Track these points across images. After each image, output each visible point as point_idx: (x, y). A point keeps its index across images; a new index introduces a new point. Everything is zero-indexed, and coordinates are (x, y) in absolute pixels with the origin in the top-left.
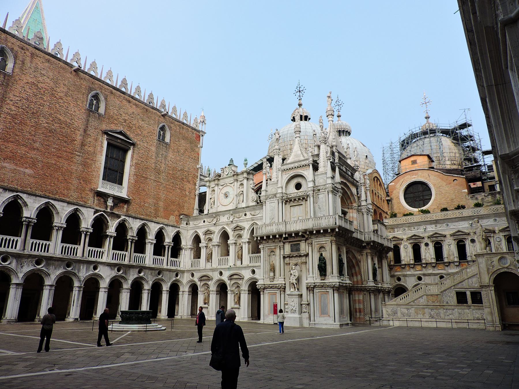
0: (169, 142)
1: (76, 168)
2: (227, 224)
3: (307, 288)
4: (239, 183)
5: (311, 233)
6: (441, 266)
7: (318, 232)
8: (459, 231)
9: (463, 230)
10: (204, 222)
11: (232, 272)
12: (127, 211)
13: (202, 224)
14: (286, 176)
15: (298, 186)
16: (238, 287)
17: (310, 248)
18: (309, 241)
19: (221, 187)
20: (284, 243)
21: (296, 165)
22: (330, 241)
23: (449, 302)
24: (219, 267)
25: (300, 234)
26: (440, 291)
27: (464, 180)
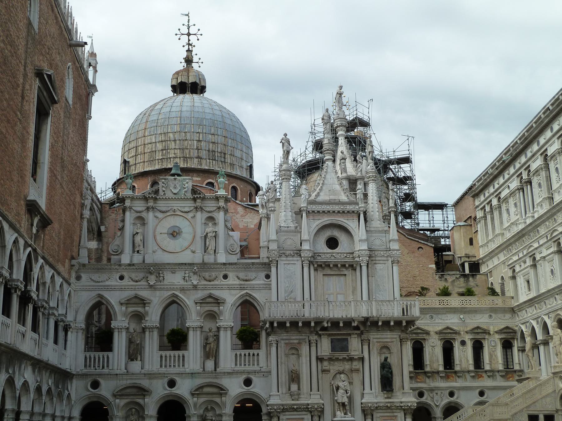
0: (71, 103)
1: (17, 146)
2: (183, 290)
3: (363, 411)
4: (206, 215)
5: (374, 324)
6: (421, 377)
7: (386, 323)
8: (448, 328)
9: (451, 327)
10: (122, 278)
11: (199, 381)
12: (43, 247)
13: (114, 281)
14: (317, 223)
15: (332, 243)
16: (212, 409)
17: (366, 347)
18: (364, 337)
19: (160, 215)
20: (320, 336)
21: (336, 208)
22: (398, 339)
24: (163, 370)
25: (356, 325)
26: (511, 414)
27: (432, 250)
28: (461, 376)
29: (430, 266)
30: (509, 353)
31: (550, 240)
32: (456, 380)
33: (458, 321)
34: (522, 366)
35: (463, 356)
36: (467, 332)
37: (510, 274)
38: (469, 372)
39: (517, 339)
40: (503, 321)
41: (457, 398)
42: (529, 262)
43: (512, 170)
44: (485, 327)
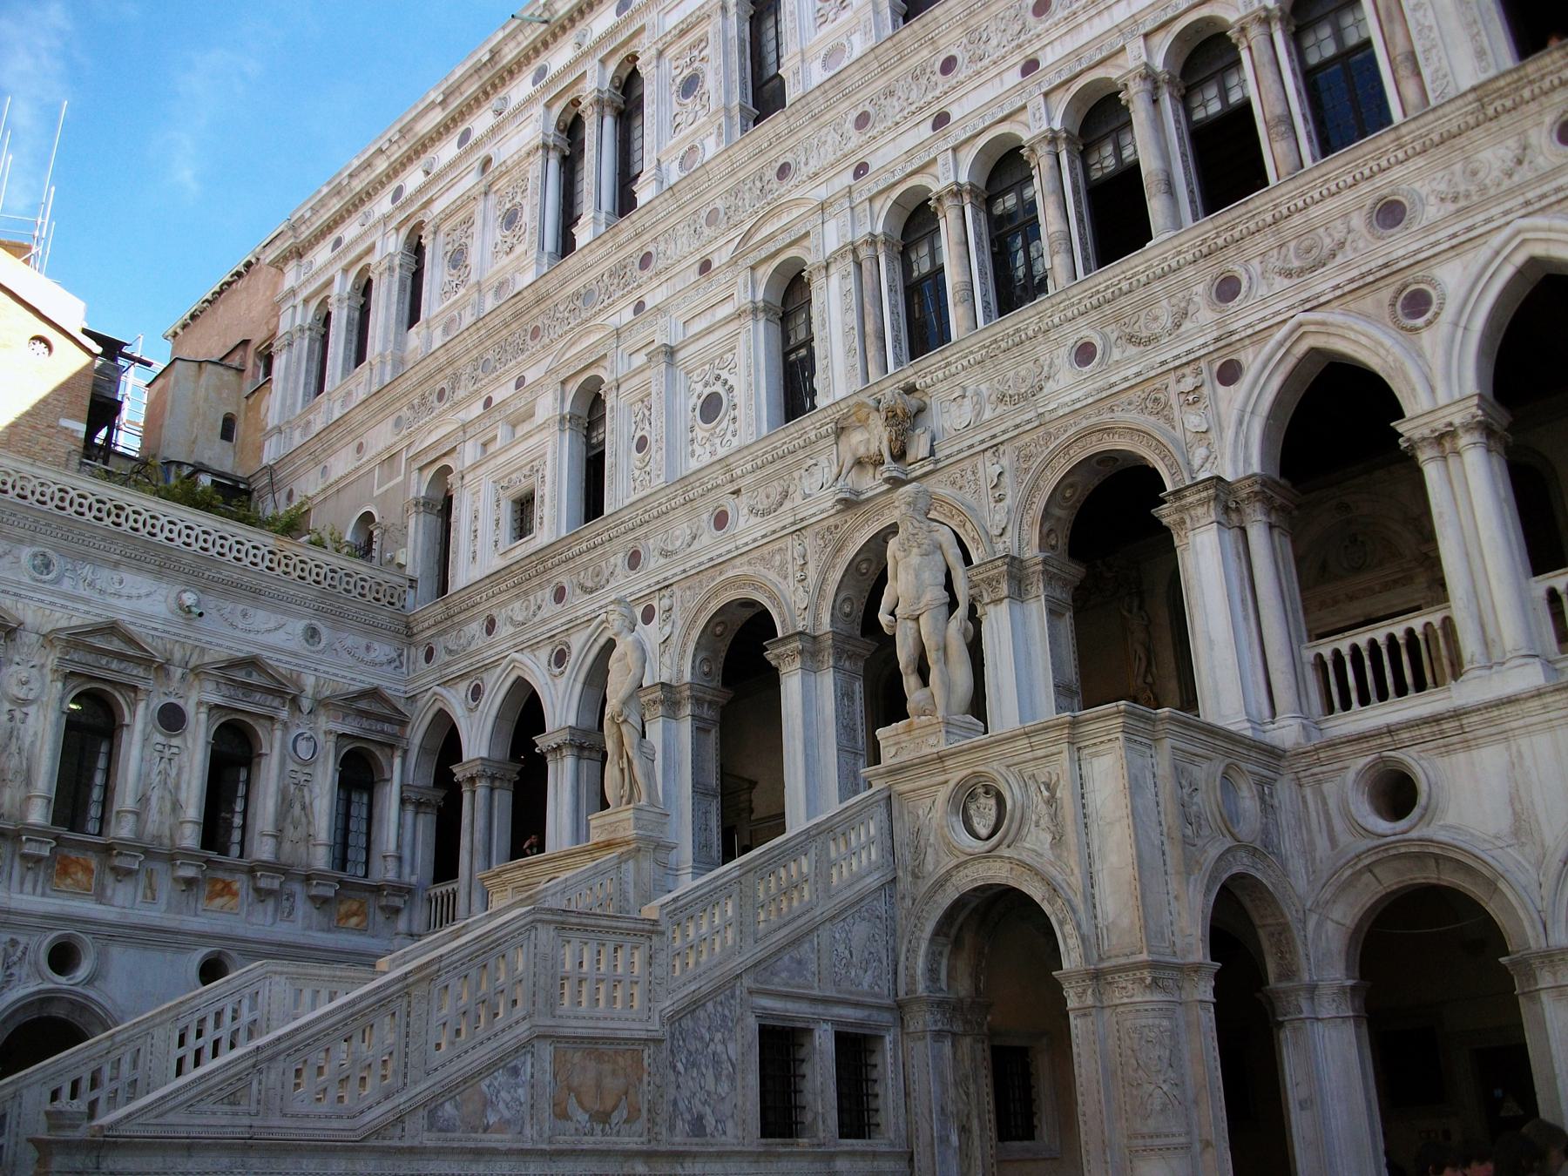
23: (710, 1121)
26: (667, 1004)
28: (129, 873)
29: (65, 423)
30: (358, 810)
31: (733, 261)
32: (103, 888)
33: (169, 616)
34: (407, 870)
35: (159, 776)
36: (198, 672)
37: (419, 486)
38: (172, 857)
39: (405, 752)
40: (362, 667)
41: (89, 981)
42: (548, 406)
43: (521, 88)
44: (282, 665)
